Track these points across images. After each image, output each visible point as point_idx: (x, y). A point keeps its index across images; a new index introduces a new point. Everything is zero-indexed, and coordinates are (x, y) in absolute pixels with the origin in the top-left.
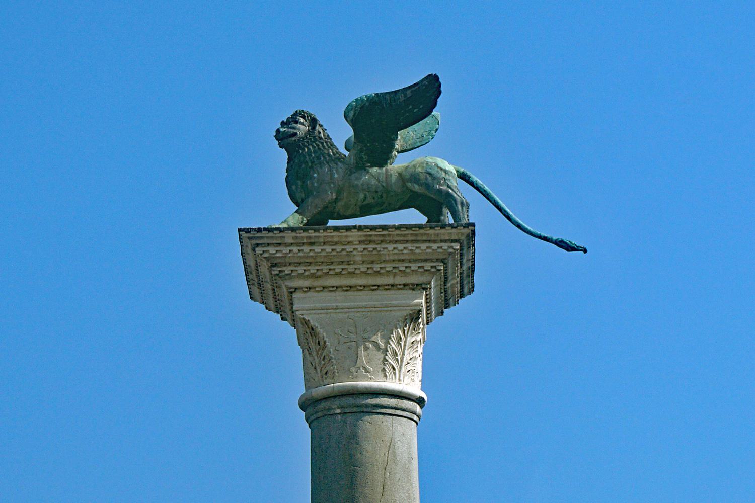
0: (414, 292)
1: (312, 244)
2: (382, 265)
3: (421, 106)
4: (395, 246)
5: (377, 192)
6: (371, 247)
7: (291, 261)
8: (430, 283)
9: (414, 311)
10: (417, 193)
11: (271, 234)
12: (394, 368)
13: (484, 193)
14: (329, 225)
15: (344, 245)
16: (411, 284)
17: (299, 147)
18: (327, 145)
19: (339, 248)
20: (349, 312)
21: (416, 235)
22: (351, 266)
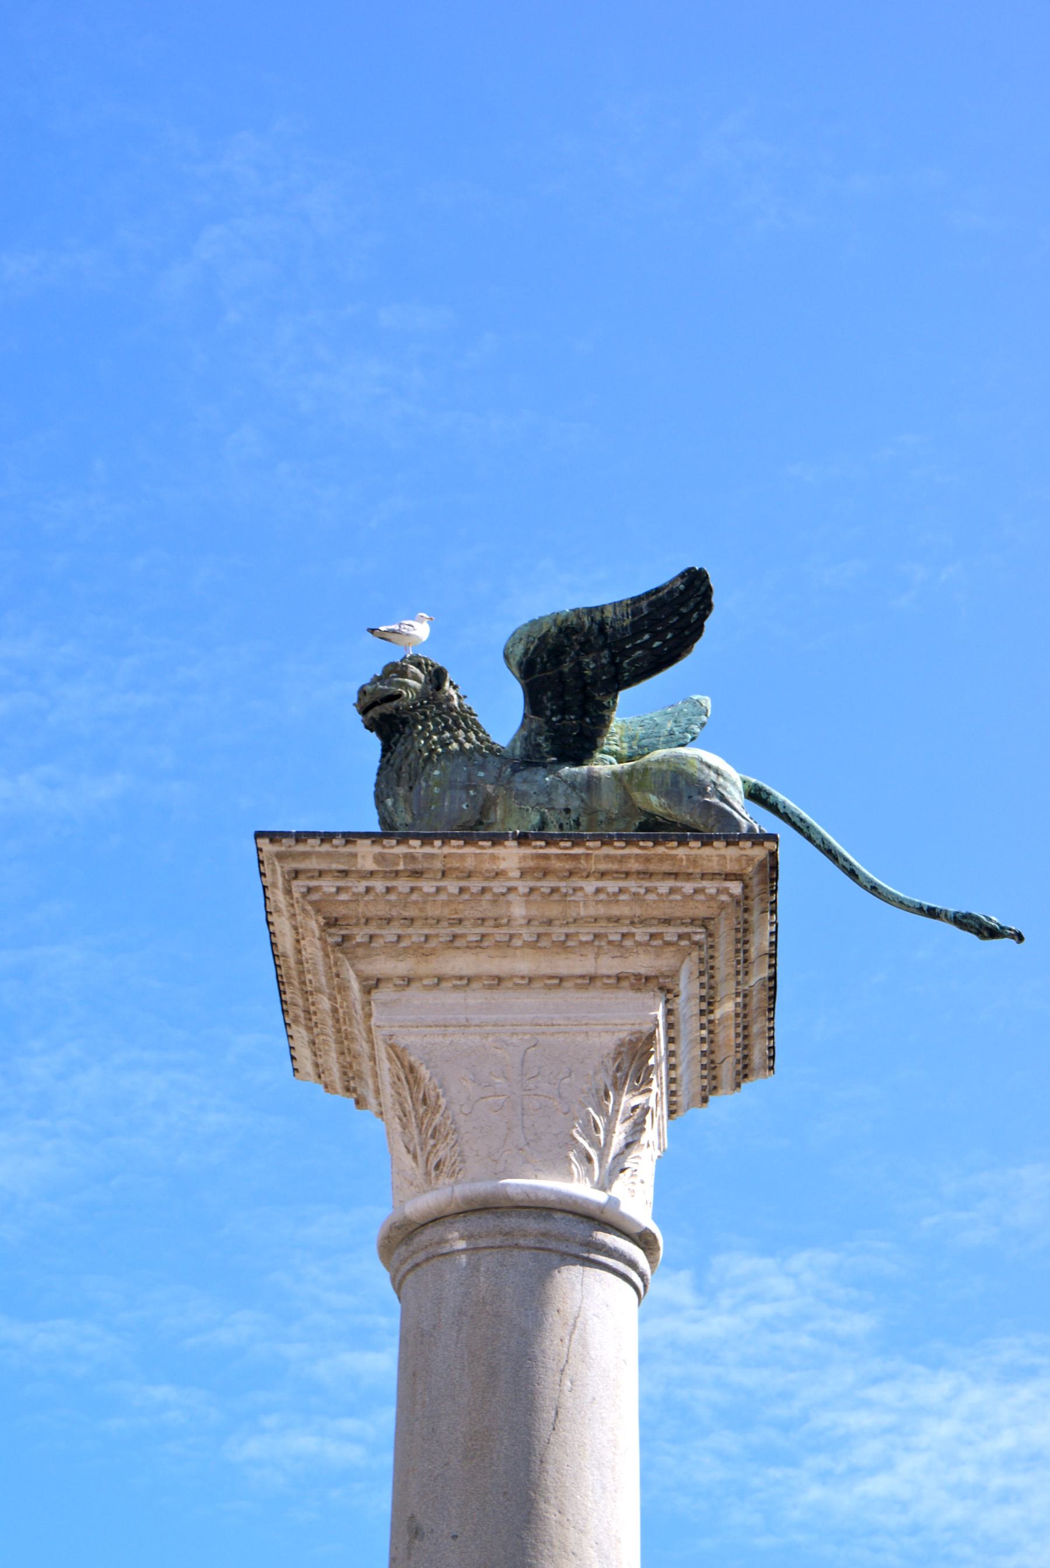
0: (639, 995)
1: (417, 874)
2: (572, 930)
3: (669, 636)
4: (600, 884)
5: (567, 811)
6: (546, 885)
7: (369, 914)
8: (674, 975)
9: (637, 1035)
10: (651, 815)
11: (326, 848)
12: (589, 1159)
13: (799, 824)
15: (487, 879)
16: (635, 975)
17: (404, 722)
18: (467, 724)
19: (475, 885)
20: (494, 1034)
21: (647, 859)
22: (504, 930)
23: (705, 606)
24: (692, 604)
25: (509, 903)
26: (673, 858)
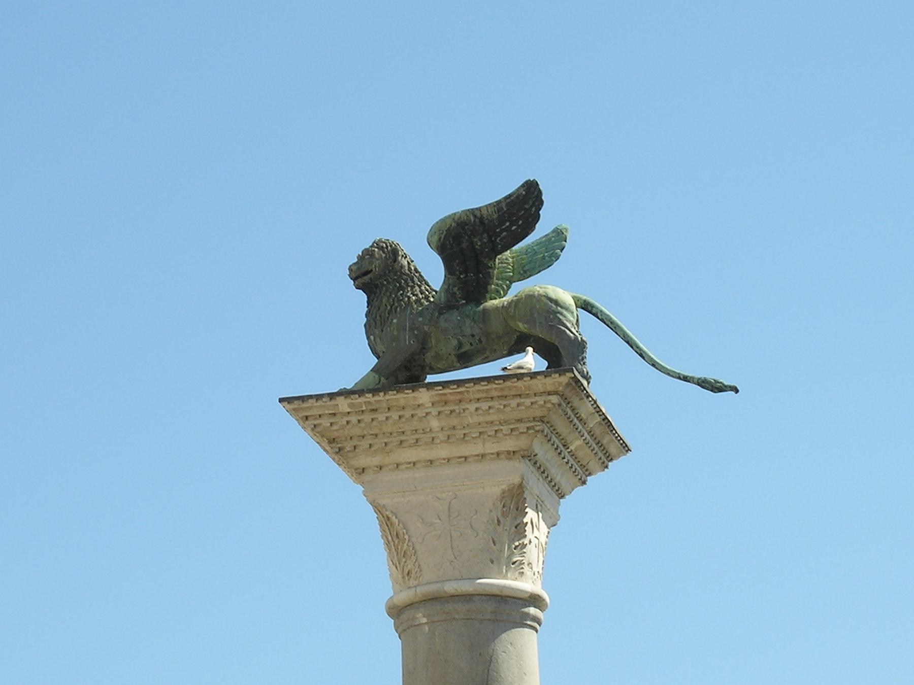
1: (375, 410)
3: (520, 222)
4: (478, 405)
5: (473, 336)
11: (320, 403)
14: (427, 381)
17: (376, 286)
19: (407, 414)
21: (502, 389)
22: (428, 435)
23: (539, 202)
24: (531, 203)
25: (429, 422)
26: (515, 387)
